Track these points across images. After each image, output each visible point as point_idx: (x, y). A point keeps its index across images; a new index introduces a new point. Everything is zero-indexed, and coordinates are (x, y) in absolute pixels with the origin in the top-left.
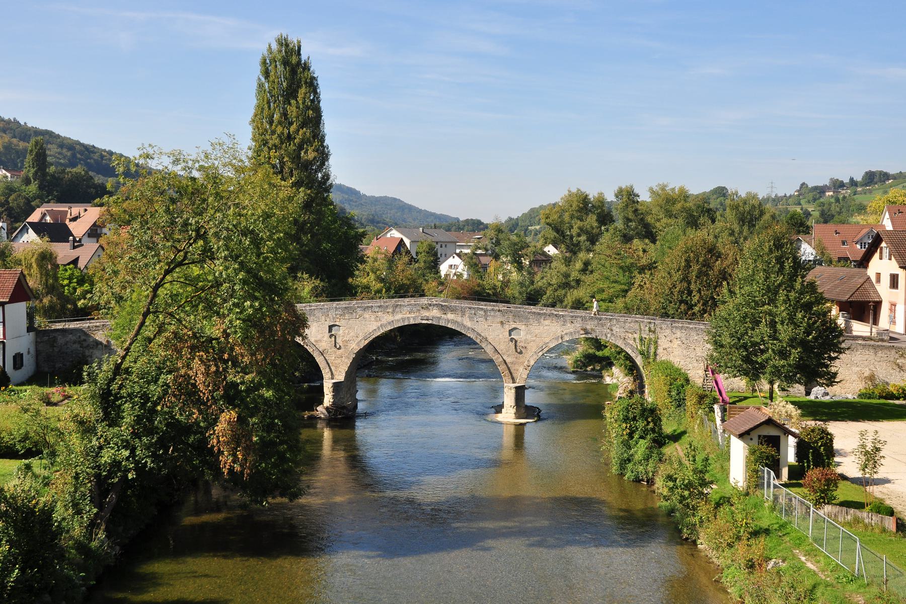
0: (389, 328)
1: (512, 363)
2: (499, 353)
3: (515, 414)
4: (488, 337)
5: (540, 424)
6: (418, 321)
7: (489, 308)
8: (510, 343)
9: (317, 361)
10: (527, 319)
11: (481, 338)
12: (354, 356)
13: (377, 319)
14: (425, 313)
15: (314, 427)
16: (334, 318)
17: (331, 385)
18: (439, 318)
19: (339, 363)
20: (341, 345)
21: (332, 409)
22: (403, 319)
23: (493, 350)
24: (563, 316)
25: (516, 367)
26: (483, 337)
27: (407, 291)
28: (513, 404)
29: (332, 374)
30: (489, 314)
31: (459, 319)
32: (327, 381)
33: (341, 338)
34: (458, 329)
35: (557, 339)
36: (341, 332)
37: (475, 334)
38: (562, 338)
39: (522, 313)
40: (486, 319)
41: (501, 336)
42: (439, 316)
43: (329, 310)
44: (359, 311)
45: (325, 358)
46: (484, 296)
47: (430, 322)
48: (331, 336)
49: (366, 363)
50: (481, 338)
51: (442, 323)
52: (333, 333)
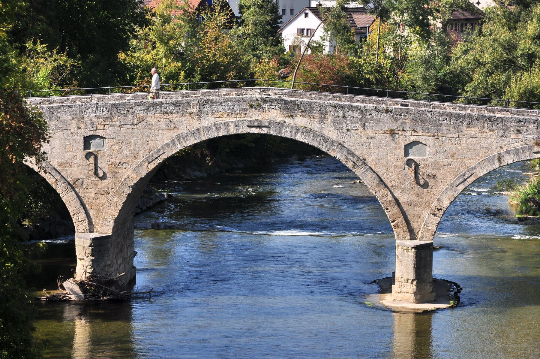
0: (193, 141)
1: (410, 204)
2: (386, 186)
3: (415, 293)
4: (367, 157)
5: (458, 312)
6: (244, 129)
7: (370, 106)
8: (407, 168)
9: (64, 199)
11: (355, 160)
12: (130, 191)
13: (171, 125)
14: (256, 116)
15: (58, 317)
16: (93, 124)
17: (88, 243)
18: (281, 125)
19: (103, 204)
20: (106, 171)
21: (91, 285)
22: (217, 127)
23: (376, 181)
24: (502, 120)
25: (417, 211)
26: (358, 157)
27: (222, 76)
28: (412, 276)
29: (90, 223)
30: (368, 116)
31: (316, 126)
32: (81, 235)
33: (106, 159)
34: (315, 144)
35: (491, 161)
36: (106, 148)
38: (499, 159)
39: (428, 114)
40: (364, 126)
41: (390, 156)
42: (280, 120)
43: (83, 109)
44: (139, 112)
45: (77, 194)
46: (360, 85)
47: (265, 131)
48: (88, 156)
49: (151, 204)
50: (355, 160)
51: (286, 133)
52: (92, 150)
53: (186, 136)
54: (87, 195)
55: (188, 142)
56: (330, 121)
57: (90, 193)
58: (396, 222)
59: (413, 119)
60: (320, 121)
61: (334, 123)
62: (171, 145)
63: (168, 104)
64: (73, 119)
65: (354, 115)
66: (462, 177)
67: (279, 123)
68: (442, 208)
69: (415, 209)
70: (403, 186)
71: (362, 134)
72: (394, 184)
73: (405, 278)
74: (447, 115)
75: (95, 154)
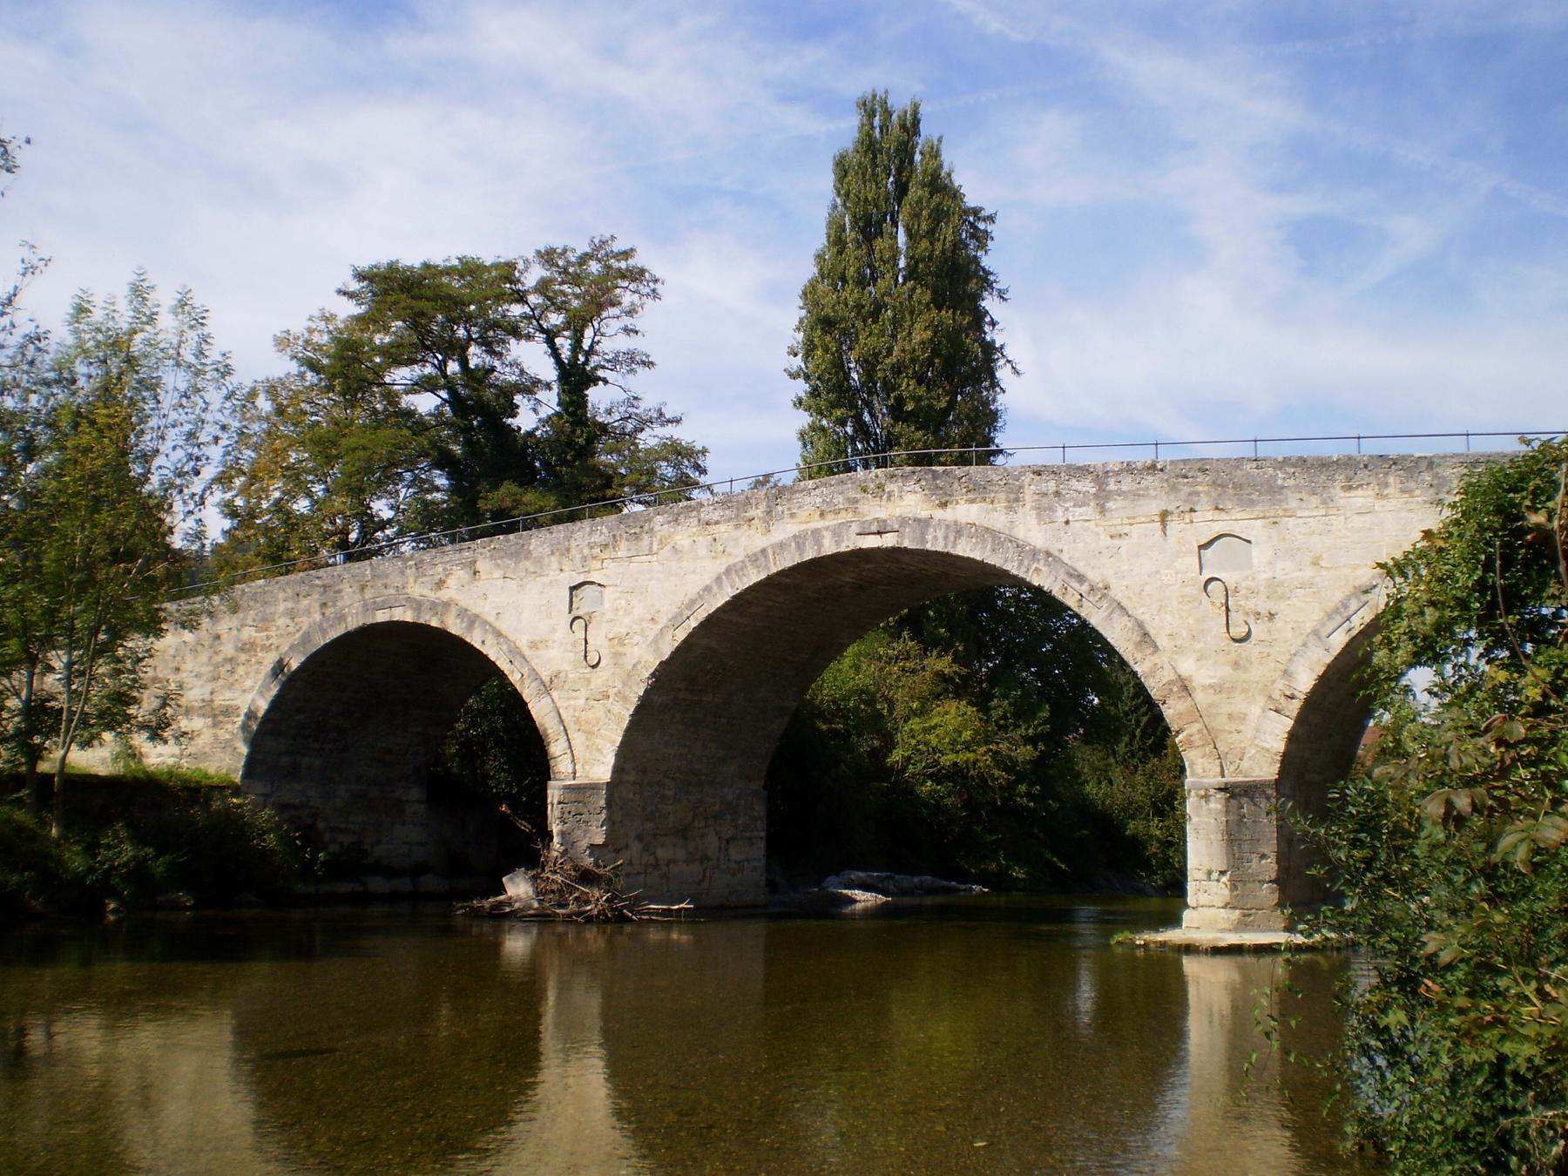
0: (755, 577)
4: (1113, 583)
10: (1274, 491)
11: (1084, 589)
16: (584, 559)
18: (923, 524)
20: (604, 652)
22: (799, 540)
25: (1238, 704)
30: (1112, 487)
31: (997, 518)
34: (994, 560)
37: (1062, 576)
40: (1103, 510)
42: (924, 514)
47: (888, 541)
53: (742, 569)
54: (572, 702)
55: (745, 579)
56: (1028, 506)
57: (575, 698)
58: (1185, 733)
59: (1214, 482)
60: (1006, 507)
61: (1039, 509)
62: (715, 588)
63: (712, 504)
64: (553, 553)
65: (1080, 488)
66: (1341, 614)
67: (919, 520)
68: (1297, 694)
69: (1232, 701)
70: (1200, 645)
71: (1101, 530)
72: (1179, 643)
73: (1207, 866)
74: (1294, 465)
75: (587, 618)
